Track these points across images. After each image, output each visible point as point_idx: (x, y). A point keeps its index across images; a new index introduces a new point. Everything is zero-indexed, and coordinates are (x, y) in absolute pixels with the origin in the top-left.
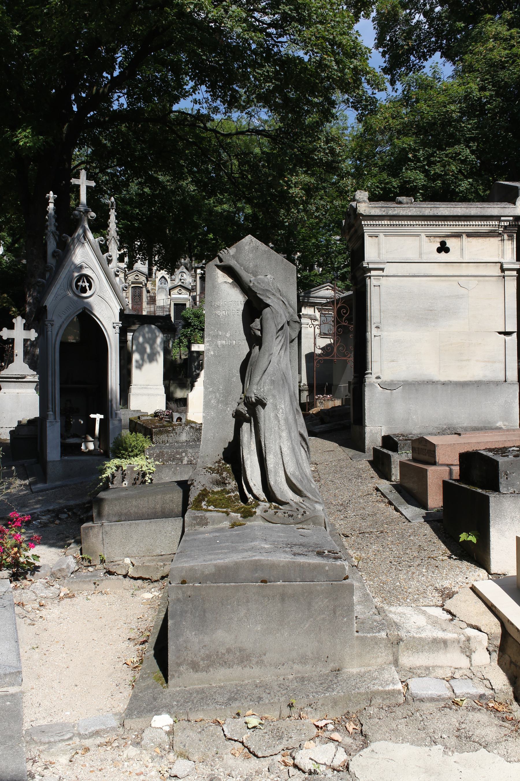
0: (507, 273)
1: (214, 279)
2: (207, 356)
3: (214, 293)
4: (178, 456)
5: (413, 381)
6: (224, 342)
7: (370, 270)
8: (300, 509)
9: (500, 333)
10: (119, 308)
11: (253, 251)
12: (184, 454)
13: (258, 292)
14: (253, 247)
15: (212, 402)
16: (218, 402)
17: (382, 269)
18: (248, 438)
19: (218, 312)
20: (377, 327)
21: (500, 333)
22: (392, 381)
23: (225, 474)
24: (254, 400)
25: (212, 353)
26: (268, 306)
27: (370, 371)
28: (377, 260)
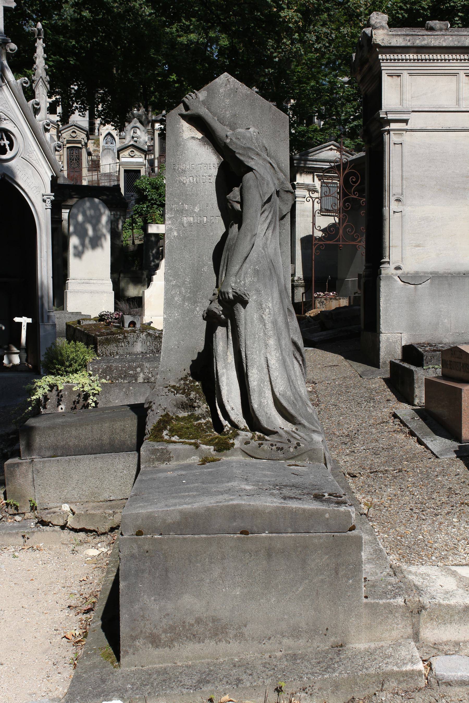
1: (178, 134)
2: (168, 238)
3: (178, 153)
4: (131, 372)
5: (445, 273)
7: (389, 122)
8: (292, 439)
10: (50, 175)
11: (230, 95)
12: (139, 370)
14: (231, 89)
15: (176, 299)
16: (184, 300)
17: (406, 121)
18: (224, 347)
19: (183, 179)
20: (398, 200)
22: (417, 273)
23: (193, 395)
24: (231, 296)
25: (176, 234)
26: (250, 169)
27: (387, 259)
28: (399, 108)
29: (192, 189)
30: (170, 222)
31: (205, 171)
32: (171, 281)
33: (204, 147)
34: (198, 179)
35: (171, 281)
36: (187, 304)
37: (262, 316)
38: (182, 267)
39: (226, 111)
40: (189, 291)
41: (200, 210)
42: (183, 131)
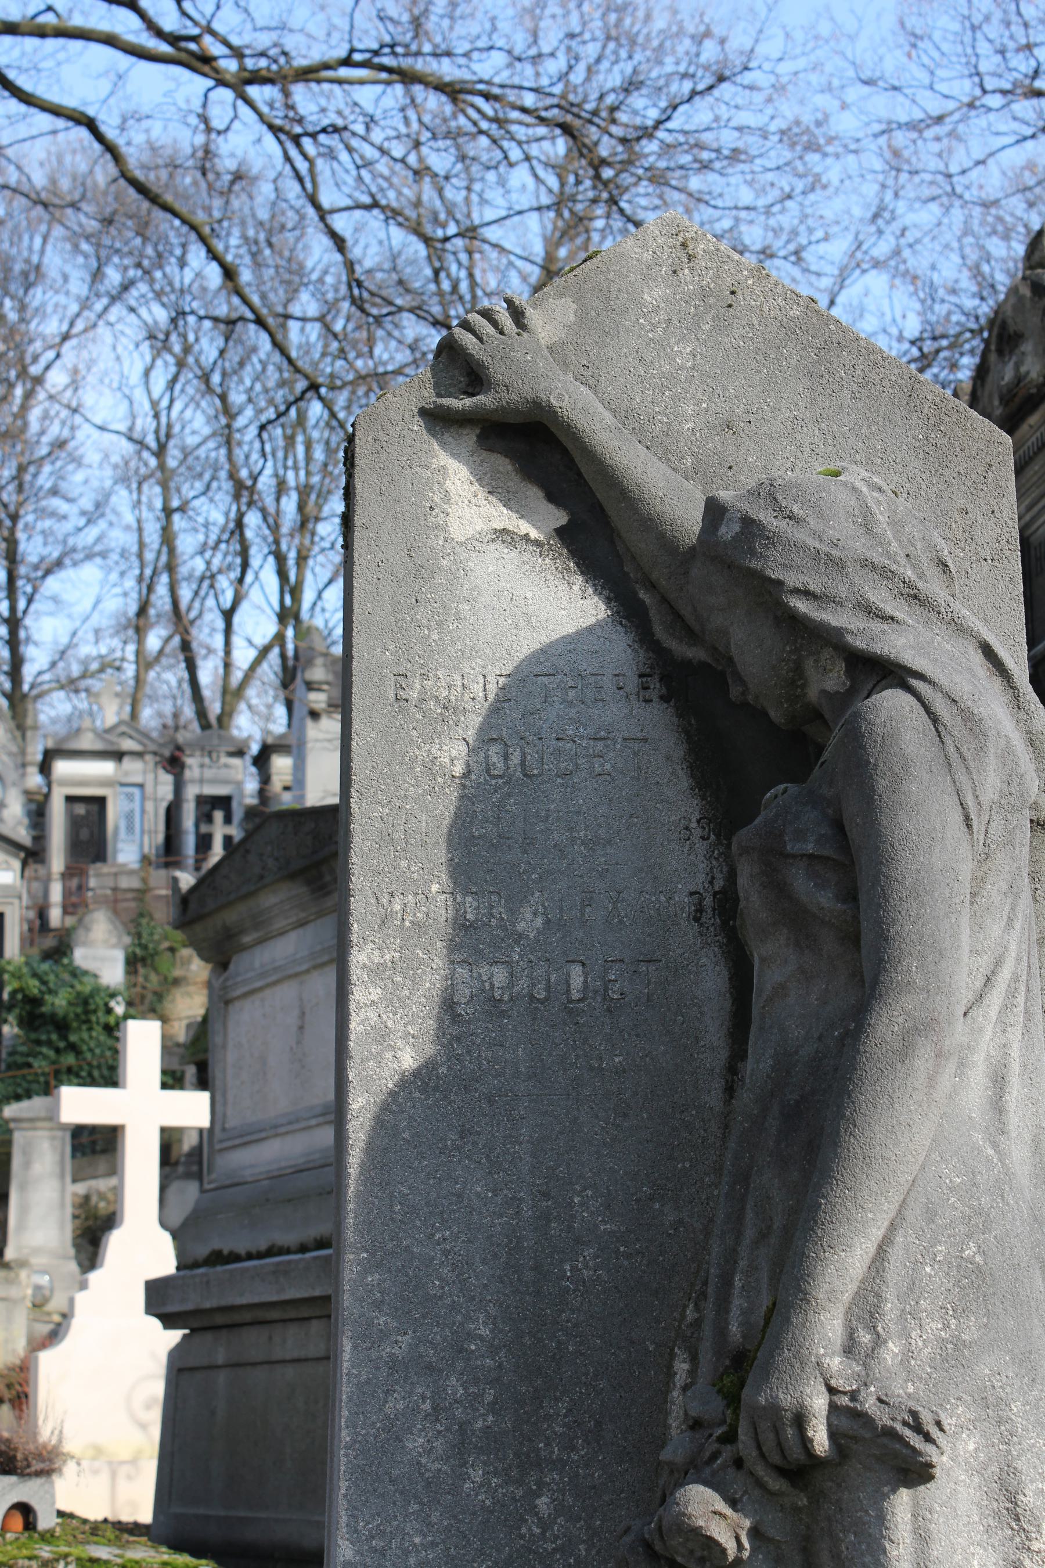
1: (424, 515)
6: (500, 976)
13: (791, 579)
14: (704, 293)
15: (415, 1443)
16: (461, 1446)
24: (820, 1438)
26: (891, 673)
29: (501, 805)
30: (375, 993)
31: (573, 713)
32: (384, 1335)
33: (563, 586)
34: (532, 757)
35: (384, 1335)
36: (477, 1474)
38: (446, 1253)
39: (677, 398)
40: (488, 1398)
41: (548, 922)
42: (447, 498)
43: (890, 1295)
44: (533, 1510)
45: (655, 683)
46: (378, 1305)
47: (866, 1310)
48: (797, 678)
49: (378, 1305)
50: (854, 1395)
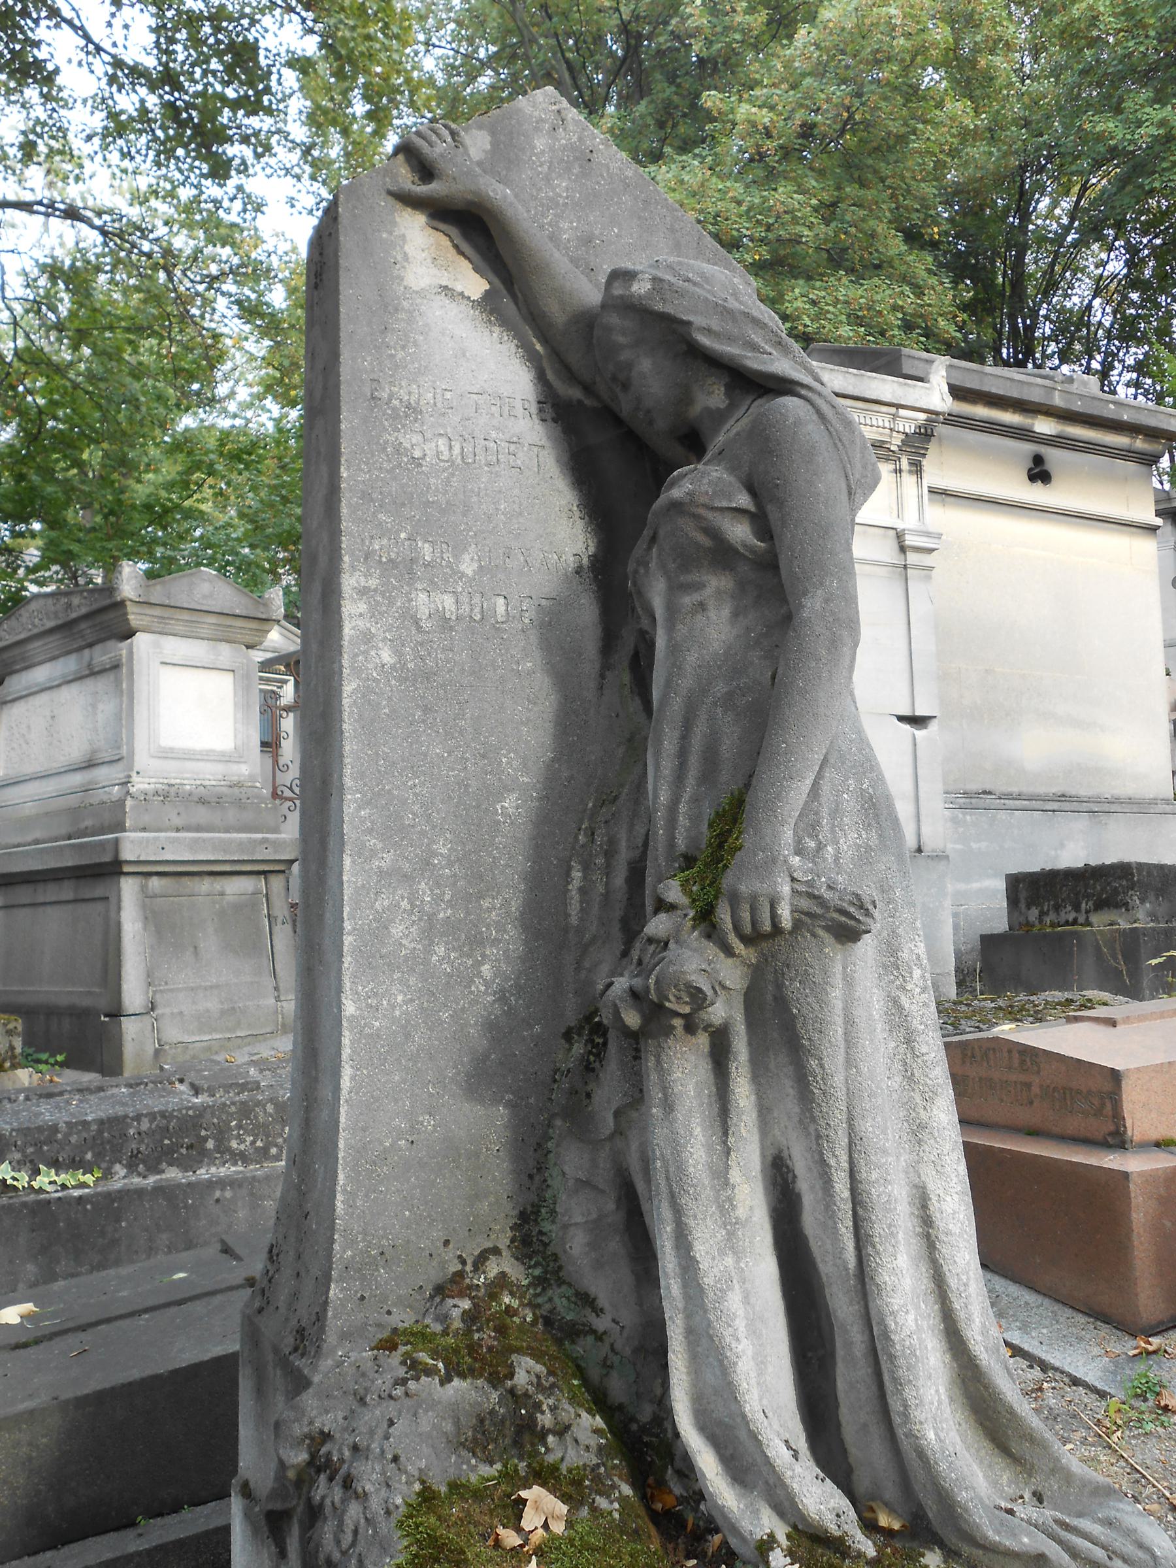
0: (912, 558)
2: (357, 671)
3: (391, 339)
6: (448, 602)
9: (901, 719)
13: (698, 320)
15: (397, 930)
16: (430, 930)
18: (709, 1148)
19: (409, 439)
21: (901, 719)
23: (525, 1371)
25: (386, 656)
29: (447, 482)
30: (363, 607)
31: (495, 422)
32: (374, 853)
33: (487, 333)
34: (469, 449)
35: (374, 853)
36: (441, 950)
37: (896, 1002)
38: (416, 795)
40: (447, 897)
41: (481, 567)
43: (825, 812)
44: (479, 974)
45: (547, 407)
46: (370, 831)
47: (809, 823)
48: (685, 398)
49: (370, 831)
50: (810, 884)
